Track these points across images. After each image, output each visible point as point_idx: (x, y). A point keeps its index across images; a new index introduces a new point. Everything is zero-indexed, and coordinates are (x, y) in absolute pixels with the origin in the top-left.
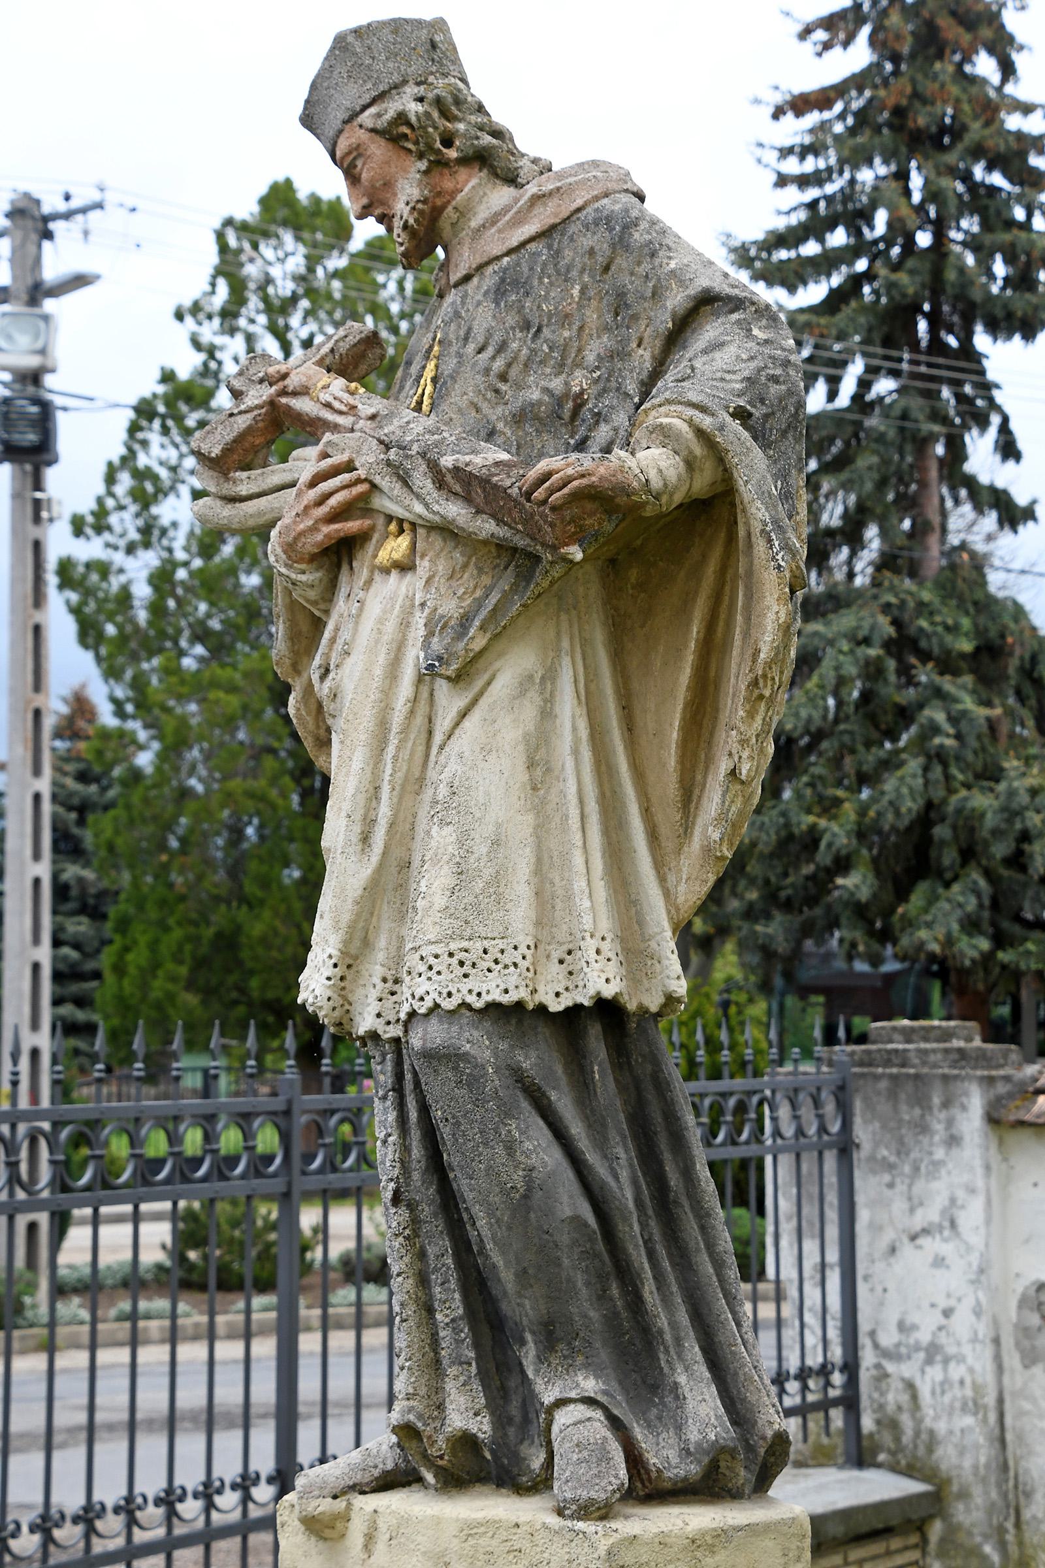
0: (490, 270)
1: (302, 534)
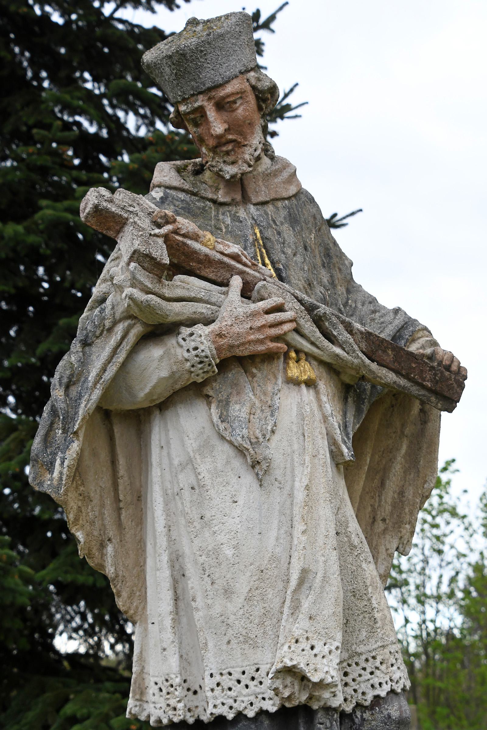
0: (280, 204)
1: (249, 342)
